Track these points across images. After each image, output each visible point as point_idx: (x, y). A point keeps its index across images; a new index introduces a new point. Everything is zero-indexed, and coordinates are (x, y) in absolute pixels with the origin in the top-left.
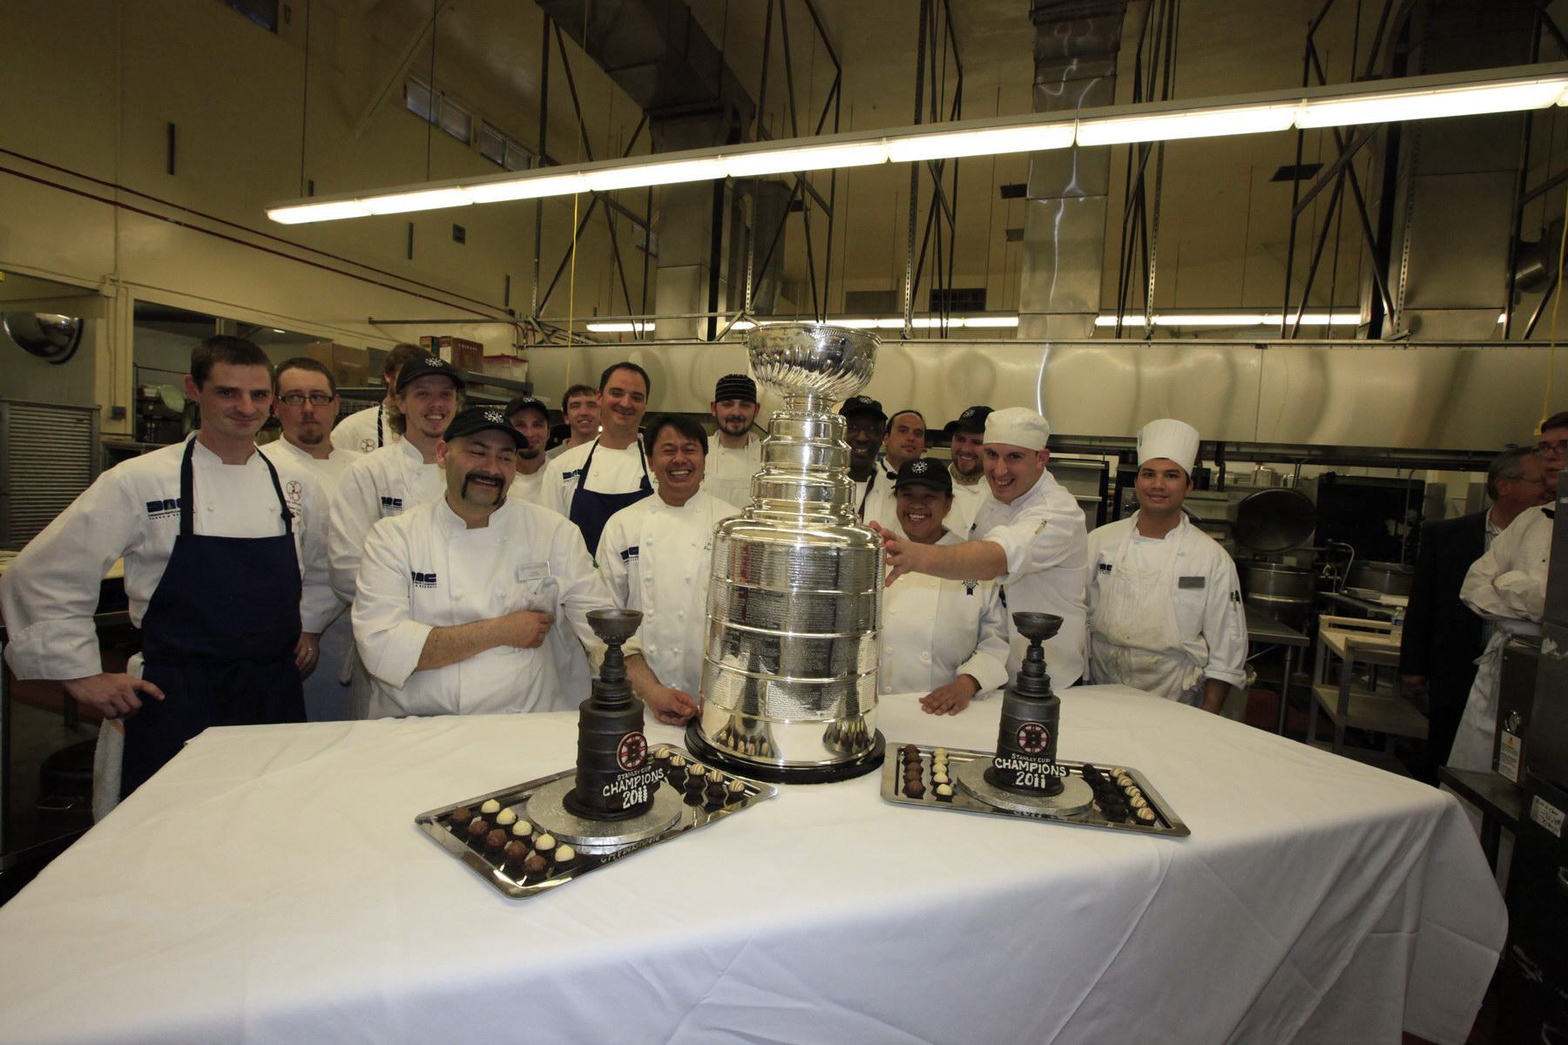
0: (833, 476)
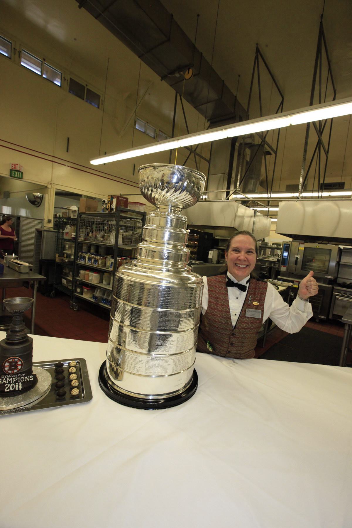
0: (175, 247)
